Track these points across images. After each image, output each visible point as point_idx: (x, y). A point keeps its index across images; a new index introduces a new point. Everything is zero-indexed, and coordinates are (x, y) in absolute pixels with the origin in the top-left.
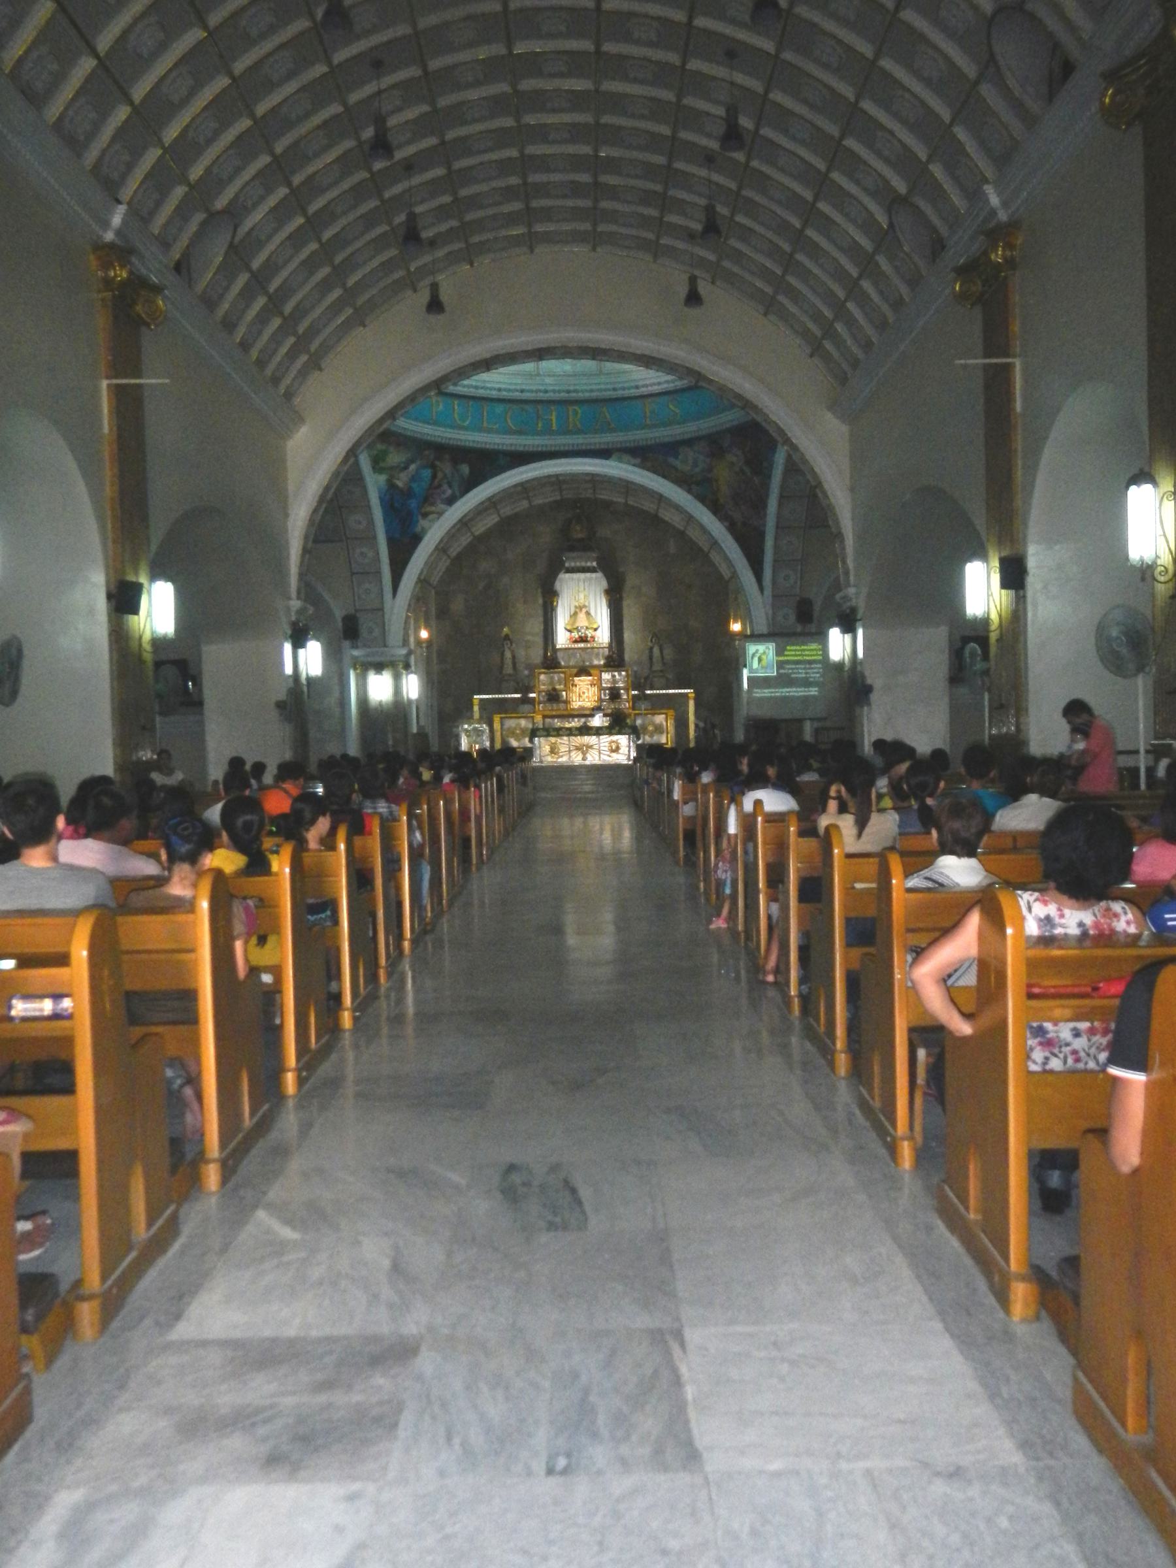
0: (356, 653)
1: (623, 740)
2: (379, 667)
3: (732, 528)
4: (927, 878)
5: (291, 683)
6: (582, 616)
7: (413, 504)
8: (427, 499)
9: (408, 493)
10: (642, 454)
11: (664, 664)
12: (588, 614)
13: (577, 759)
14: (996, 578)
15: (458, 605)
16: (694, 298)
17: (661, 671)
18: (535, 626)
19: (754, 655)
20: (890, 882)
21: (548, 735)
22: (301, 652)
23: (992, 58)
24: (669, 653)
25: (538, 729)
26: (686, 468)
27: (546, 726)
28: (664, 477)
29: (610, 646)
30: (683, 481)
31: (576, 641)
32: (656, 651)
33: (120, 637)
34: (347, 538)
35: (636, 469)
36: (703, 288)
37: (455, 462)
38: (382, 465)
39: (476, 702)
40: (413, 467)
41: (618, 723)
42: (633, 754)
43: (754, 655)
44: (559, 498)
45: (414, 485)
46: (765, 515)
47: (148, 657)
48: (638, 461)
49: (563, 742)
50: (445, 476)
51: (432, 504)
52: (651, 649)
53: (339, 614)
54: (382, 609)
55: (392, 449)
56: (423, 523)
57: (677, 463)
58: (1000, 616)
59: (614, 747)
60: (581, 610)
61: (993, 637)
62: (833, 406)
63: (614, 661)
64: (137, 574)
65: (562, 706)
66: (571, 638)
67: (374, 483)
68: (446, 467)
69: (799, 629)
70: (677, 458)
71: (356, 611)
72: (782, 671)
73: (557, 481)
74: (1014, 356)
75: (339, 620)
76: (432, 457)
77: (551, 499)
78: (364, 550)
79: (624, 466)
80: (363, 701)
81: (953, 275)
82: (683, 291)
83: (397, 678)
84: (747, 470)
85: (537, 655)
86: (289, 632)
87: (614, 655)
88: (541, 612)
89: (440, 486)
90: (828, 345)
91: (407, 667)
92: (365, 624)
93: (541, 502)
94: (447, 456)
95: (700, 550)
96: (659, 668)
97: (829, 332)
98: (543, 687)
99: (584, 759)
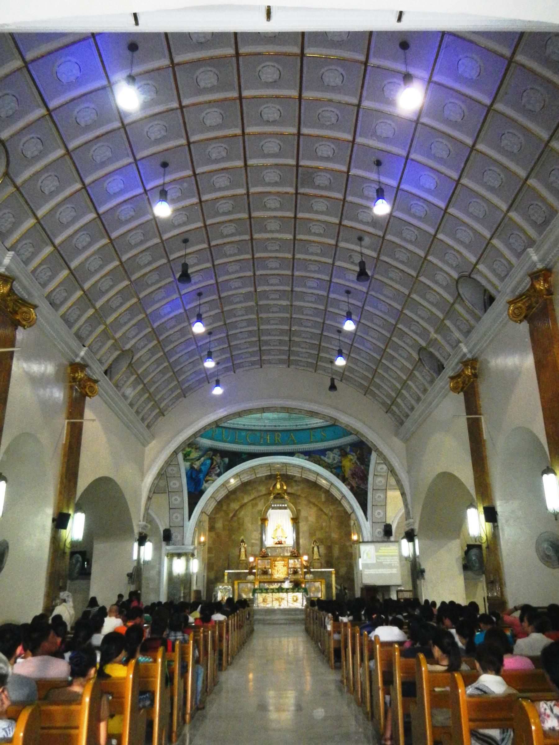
0: (168, 548)
1: (299, 595)
2: (179, 555)
3: (352, 489)
4: (478, 689)
5: (135, 564)
6: (279, 531)
7: (201, 476)
8: (208, 474)
9: (199, 471)
10: (309, 455)
11: (320, 556)
12: (282, 529)
13: (276, 605)
14: (483, 517)
15: (219, 525)
16: (333, 387)
17: (318, 559)
18: (256, 535)
20: (458, 691)
21: (262, 592)
22: (142, 548)
23: (459, 294)
24: (322, 550)
25: (256, 589)
26: (330, 461)
27: (261, 587)
28: (319, 465)
29: (293, 548)
30: (328, 467)
31: (276, 544)
32: (316, 549)
33: (55, 540)
34: (169, 492)
35: (307, 462)
36: (336, 383)
37: (222, 457)
38: (188, 458)
40: (202, 459)
41: (297, 586)
42: (305, 603)
44: (269, 474)
45: (203, 468)
46: (367, 483)
47: (68, 551)
48: (307, 457)
49: (269, 596)
50: (217, 464)
51: (210, 476)
52: (313, 548)
53: (162, 529)
54: (183, 526)
55: (193, 450)
56: (205, 485)
57: (326, 459)
58: (487, 536)
59: (295, 599)
61: (484, 546)
62: (397, 435)
64: (68, 509)
65: (269, 577)
67: (184, 466)
68: (217, 459)
69: (386, 540)
70: (325, 457)
71: (170, 526)
72: (378, 560)
73: (269, 465)
74: (480, 414)
75: (162, 532)
76: (211, 455)
77: (266, 474)
78: (178, 498)
79: (300, 460)
80: (170, 573)
81: (449, 379)
82: (329, 384)
83: (188, 561)
84: (359, 463)
85: (257, 549)
86: (137, 537)
88: (260, 529)
89: (214, 468)
90: (394, 408)
91: (193, 555)
93: (261, 475)
94: (218, 454)
95: (337, 499)
96: (317, 558)
97: (394, 402)
98: (259, 567)
99: (280, 605)
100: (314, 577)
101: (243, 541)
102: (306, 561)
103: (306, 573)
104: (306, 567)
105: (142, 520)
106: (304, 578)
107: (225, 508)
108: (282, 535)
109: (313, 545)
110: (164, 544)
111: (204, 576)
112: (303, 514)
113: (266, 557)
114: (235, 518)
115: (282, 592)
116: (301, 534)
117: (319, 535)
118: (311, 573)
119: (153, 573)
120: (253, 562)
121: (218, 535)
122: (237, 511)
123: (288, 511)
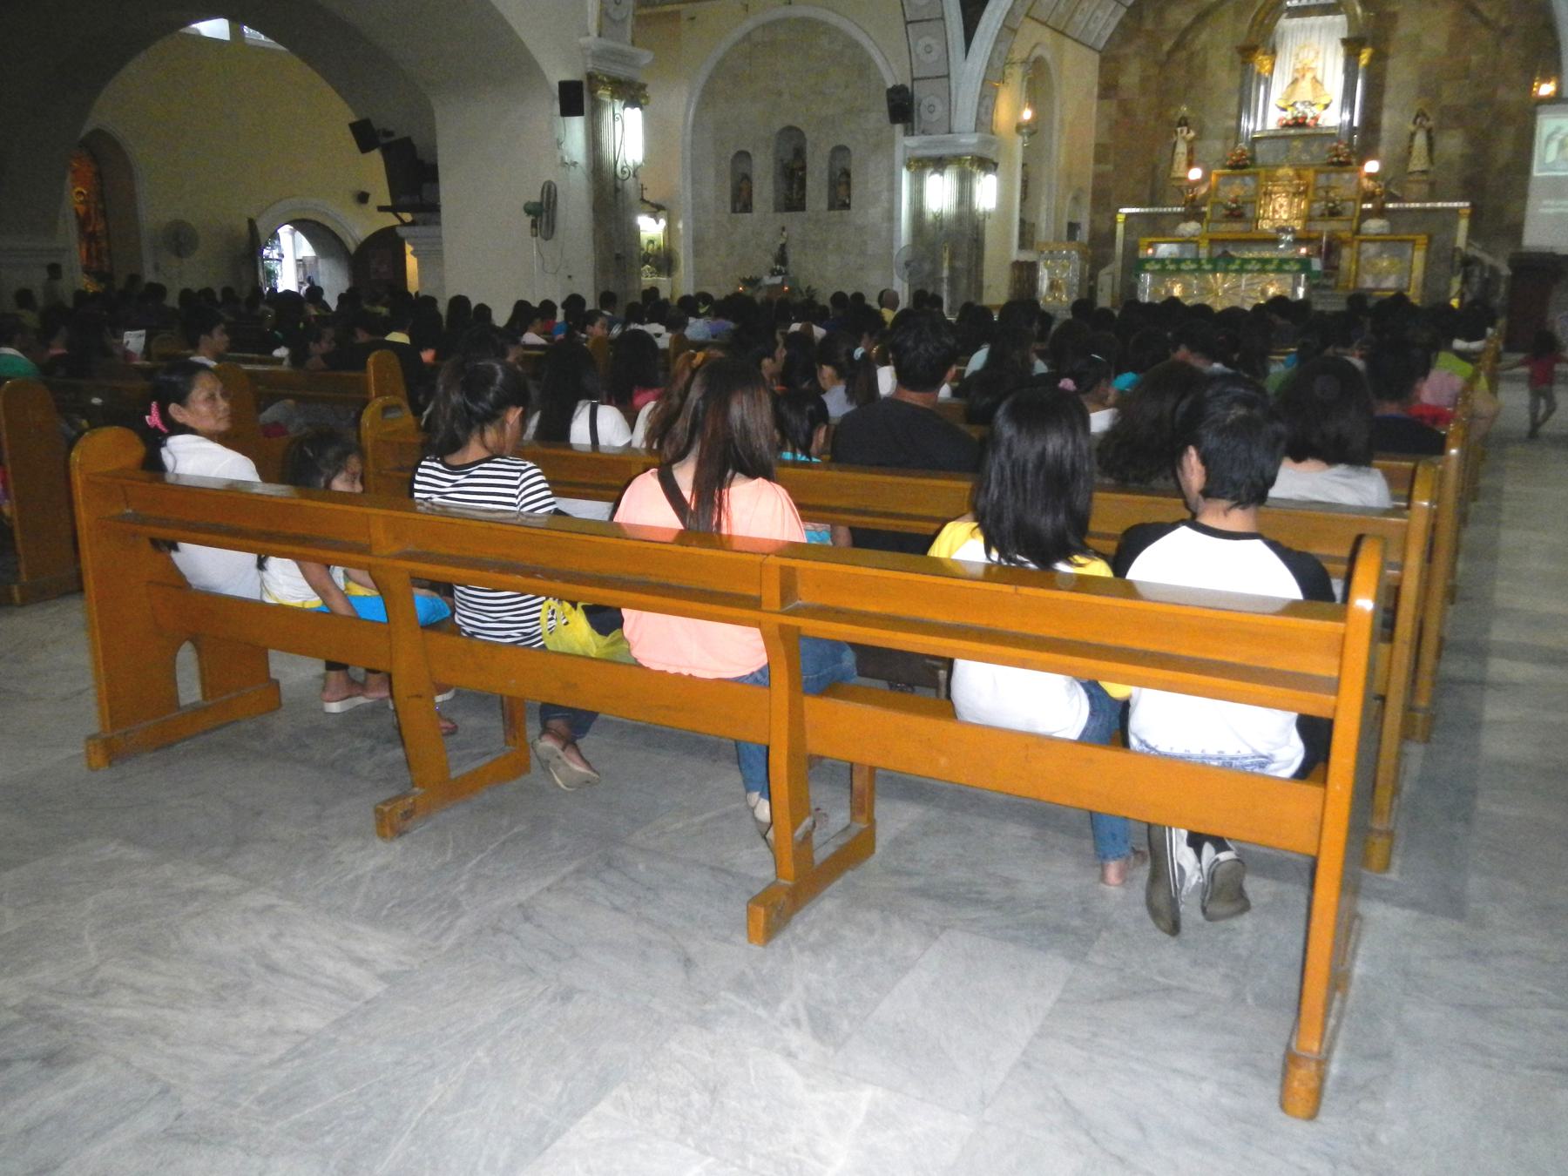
0: (911, 142)
2: (939, 164)
6: (1305, 87)
15: (1131, 77)
17: (1423, 172)
19: (1550, 138)
24: (1453, 144)
31: (1287, 126)
32: (1420, 140)
39: (1120, 218)
43: (1550, 138)
52: (1413, 135)
53: (890, 85)
54: (948, 76)
60: (1303, 76)
63: (1338, 156)
66: (1280, 120)
80: (918, 213)
87: (1341, 146)
91: (986, 164)
92: (924, 95)
96: (1424, 168)
100: (1393, 224)
101: (1184, 122)
102: (1371, 176)
103: (1366, 215)
104: (1369, 196)
105: (593, 26)
106: (1358, 231)
107: (1149, 25)
108: (1309, 98)
109: (1412, 128)
110: (899, 128)
111: (1073, 228)
112: (1406, 27)
113: (1245, 166)
114: (1183, 55)
115: (1226, 271)
116: (1389, 97)
117: (1449, 95)
118: (1380, 212)
119: (875, 213)
120: (1197, 183)
121: (1125, 109)
122: (1187, 30)
123: (1340, 20)
